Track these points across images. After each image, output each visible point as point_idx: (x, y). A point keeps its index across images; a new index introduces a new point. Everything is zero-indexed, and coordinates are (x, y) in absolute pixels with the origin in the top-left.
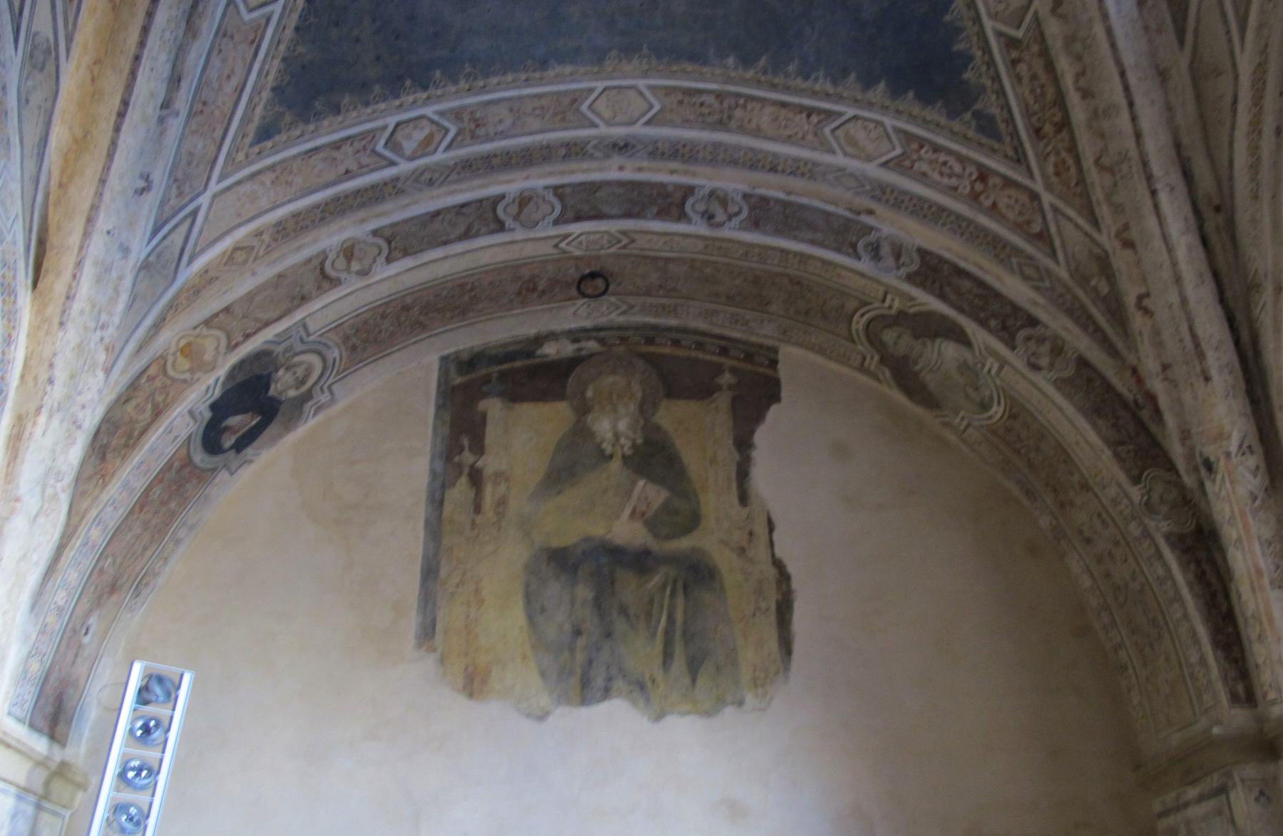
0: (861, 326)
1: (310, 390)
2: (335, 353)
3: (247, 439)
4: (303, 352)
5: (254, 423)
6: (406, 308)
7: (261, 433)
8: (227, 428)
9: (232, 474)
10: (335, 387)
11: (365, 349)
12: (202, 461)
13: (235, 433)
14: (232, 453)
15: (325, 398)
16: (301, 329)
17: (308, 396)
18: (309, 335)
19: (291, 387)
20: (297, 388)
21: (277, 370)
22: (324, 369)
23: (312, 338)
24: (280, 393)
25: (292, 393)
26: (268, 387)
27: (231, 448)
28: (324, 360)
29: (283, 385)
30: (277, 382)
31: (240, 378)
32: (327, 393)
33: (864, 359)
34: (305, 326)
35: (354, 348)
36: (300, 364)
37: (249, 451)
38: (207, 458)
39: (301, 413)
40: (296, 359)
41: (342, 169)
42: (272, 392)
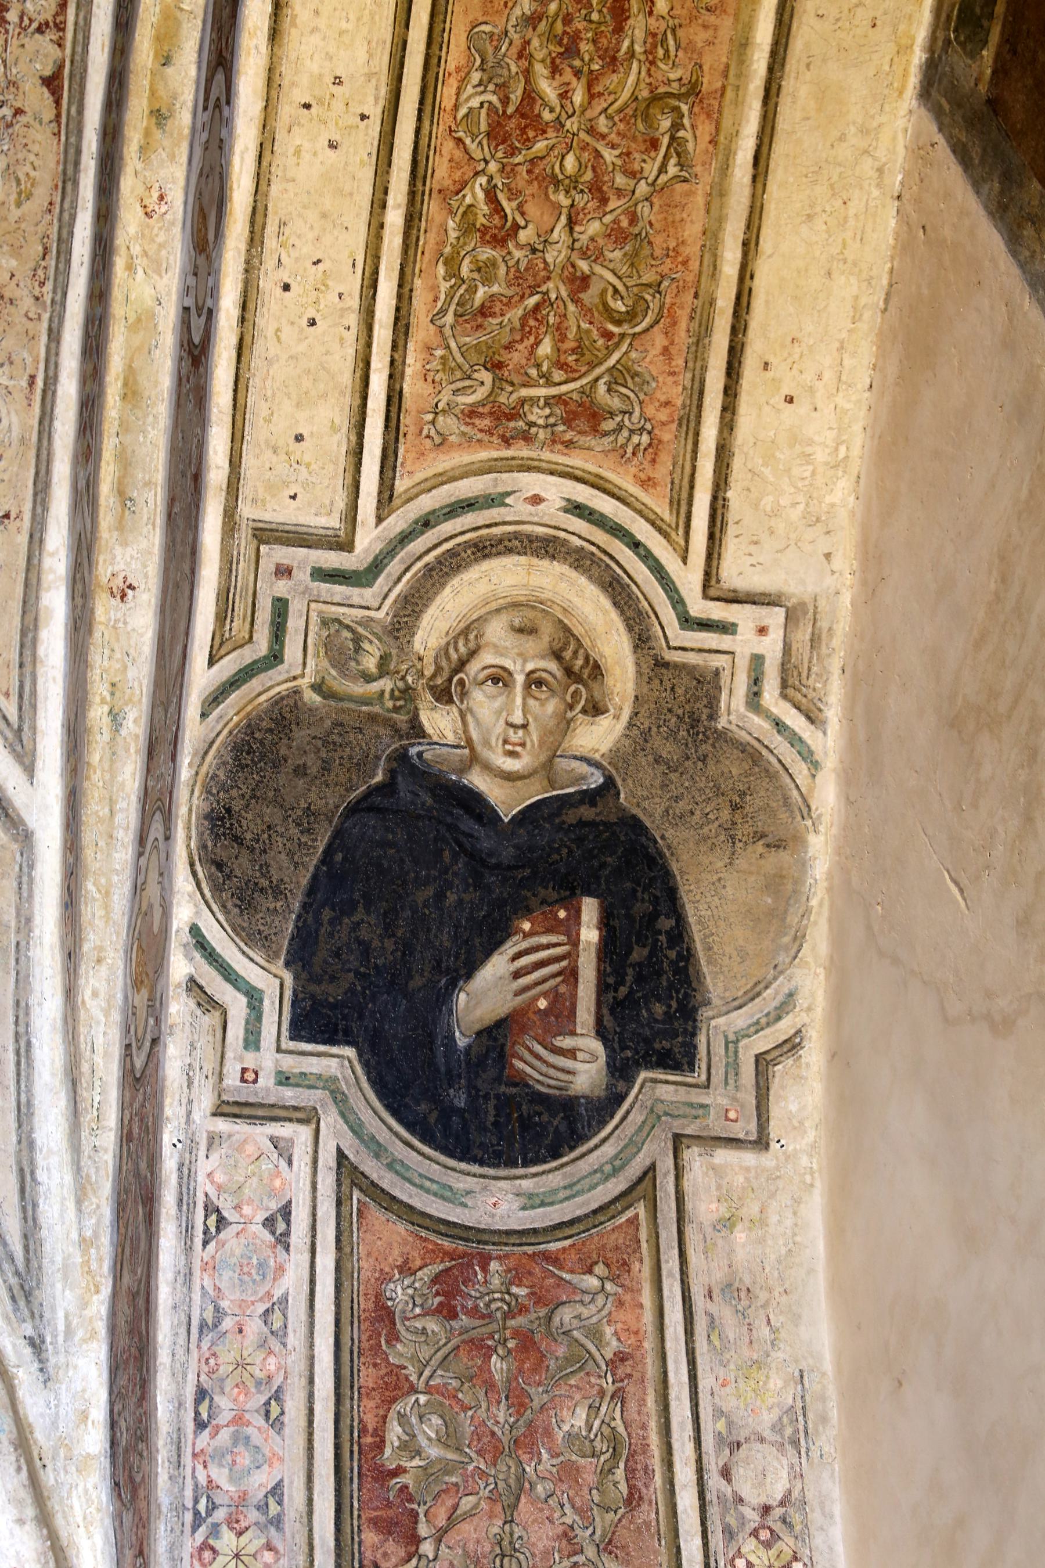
1: (656, 667)
2: (542, 496)
3: (654, 1006)
4: (412, 606)
5: (590, 935)
6: (514, 124)
7: (679, 934)
8: (497, 1036)
9: (761, 1143)
10: (735, 572)
12: (531, 1201)
13: (561, 1015)
14: (655, 1088)
15: (756, 636)
16: (275, 554)
18: (346, 545)
19: (566, 725)
20: (595, 709)
21: (417, 730)
22: (581, 560)
23: (368, 539)
26: (473, 804)
28: (547, 547)
29: (501, 746)
30: (474, 759)
32: (742, 615)
34: (266, 534)
35: (584, 416)
36: (468, 635)
38: (549, 1178)
39: (752, 754)
40: (431, 633)
41: (36, 99)
42: (505, 800)
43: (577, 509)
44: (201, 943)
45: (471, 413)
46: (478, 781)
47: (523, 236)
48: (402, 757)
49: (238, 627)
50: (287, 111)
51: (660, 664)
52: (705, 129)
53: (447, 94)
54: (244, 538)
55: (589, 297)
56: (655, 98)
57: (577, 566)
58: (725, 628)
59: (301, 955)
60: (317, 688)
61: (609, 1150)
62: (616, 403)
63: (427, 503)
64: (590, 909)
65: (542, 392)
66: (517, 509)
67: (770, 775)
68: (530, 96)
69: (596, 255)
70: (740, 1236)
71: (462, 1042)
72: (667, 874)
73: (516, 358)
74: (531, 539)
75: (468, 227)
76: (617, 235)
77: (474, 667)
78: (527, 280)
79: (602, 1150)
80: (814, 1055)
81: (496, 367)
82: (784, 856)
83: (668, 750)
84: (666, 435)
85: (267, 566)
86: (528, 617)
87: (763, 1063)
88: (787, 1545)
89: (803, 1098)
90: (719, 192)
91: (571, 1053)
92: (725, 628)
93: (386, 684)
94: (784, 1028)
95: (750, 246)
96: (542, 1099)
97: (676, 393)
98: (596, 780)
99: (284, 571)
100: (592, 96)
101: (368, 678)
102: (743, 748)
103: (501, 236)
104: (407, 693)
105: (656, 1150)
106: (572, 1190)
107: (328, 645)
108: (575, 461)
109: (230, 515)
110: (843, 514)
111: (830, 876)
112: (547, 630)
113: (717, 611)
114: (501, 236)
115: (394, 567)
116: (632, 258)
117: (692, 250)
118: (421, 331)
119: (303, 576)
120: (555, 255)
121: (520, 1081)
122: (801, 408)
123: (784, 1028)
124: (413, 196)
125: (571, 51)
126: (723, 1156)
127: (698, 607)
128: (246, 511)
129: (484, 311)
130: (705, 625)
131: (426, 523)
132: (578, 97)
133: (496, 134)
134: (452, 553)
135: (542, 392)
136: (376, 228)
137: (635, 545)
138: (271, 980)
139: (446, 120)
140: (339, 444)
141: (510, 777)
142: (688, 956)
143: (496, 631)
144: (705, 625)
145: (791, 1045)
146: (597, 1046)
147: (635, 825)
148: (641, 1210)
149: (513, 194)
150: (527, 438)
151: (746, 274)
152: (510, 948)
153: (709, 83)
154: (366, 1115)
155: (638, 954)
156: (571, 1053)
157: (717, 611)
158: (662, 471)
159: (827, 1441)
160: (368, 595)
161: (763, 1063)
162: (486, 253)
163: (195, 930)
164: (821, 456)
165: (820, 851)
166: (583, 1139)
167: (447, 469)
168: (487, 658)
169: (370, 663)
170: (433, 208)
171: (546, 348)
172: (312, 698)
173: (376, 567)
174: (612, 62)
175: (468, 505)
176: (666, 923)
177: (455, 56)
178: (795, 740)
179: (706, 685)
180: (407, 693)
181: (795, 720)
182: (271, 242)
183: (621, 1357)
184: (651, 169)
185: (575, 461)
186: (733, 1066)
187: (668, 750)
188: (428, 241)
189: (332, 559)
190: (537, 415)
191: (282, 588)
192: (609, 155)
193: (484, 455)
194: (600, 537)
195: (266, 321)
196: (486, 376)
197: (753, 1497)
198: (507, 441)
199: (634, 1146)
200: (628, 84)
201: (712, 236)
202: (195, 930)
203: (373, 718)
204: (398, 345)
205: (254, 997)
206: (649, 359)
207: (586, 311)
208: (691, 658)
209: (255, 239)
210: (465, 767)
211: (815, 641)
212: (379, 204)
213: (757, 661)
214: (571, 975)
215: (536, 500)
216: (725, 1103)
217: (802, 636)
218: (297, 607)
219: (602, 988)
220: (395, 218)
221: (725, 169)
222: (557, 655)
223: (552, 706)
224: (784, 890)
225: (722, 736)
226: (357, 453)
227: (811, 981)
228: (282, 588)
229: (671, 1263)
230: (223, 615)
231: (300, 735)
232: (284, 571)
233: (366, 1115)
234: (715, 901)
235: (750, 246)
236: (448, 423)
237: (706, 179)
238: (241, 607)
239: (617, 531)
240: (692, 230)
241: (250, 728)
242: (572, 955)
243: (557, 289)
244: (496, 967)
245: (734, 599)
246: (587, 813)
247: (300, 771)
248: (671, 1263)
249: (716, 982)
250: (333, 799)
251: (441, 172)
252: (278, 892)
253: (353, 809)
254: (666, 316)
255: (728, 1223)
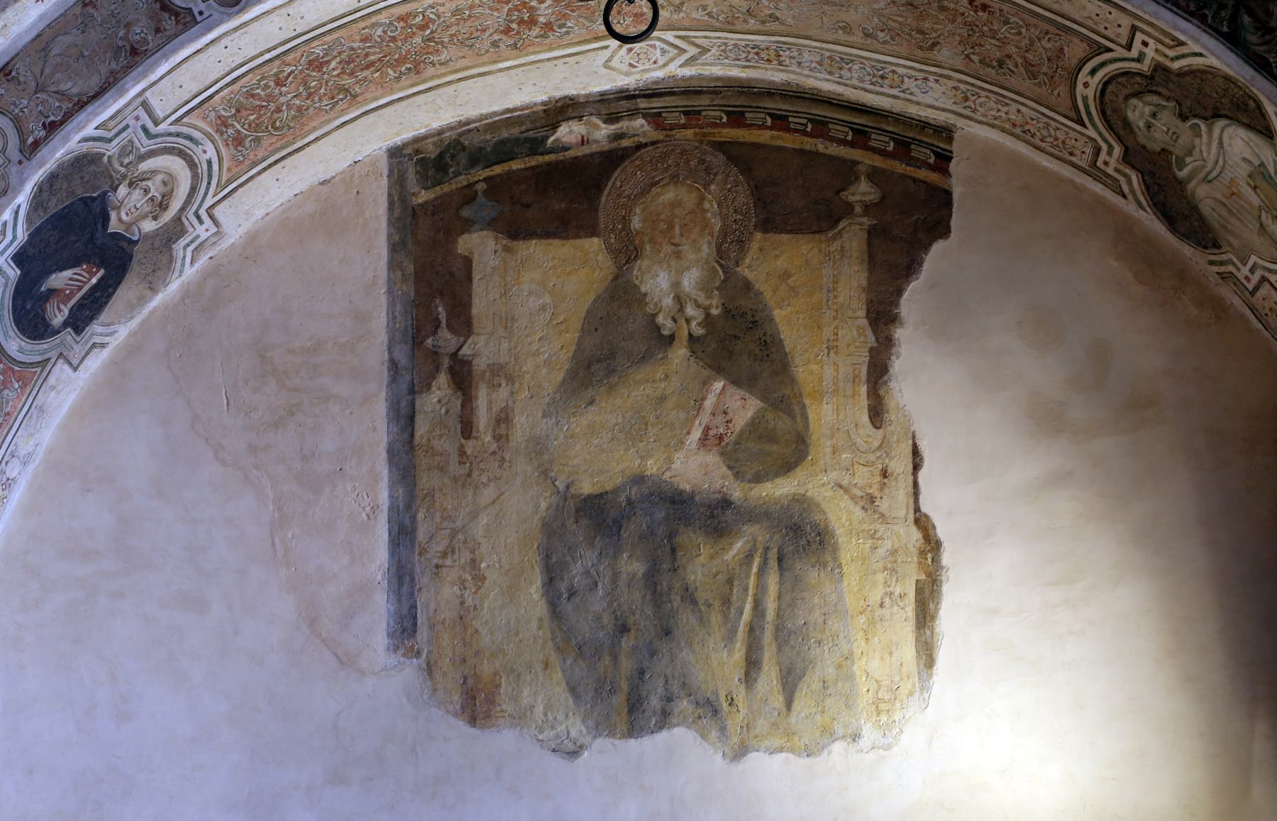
0: (1090, 93)
1: (178, 219)
3: (87, 312)
4: (152, 154)
5: (94, 281)
6: (317, 64)
7: (110, 296)
8: (52, 292)
9: (75, 369)
10: (218, 212)
11: (257, 140)
12: (21, 351)
15: (204, 230)
16: (141, 112)
17: (176, 230)
18: (156, 124)
19: (145, 217)
20: (155, 218)
21: (115, 189)
22: (195, 177)
23: (163, 127)
24: (129, 226)
25: (148, 226)
26: (106, 219)
27: (66, 324)
28: (192, 165)
29: (129, 211)
30: (118, 208)
31: (54, 207)
33: (1097, 151)
34: (145, 105)
35: (238, 141)
36: (154, 172)
37: (96, 327)
38: (27, 344)
39: (171, 260)
40: (145, 166)
42: (114, 226)
43: (209, 163)
44: (17, 213)
45: (219, 117)
46: (113, 215)
47: (284, 89)
48: (105, 193)
49: (112, 123)
50: (284, 11)
51: (180, 219)
52: (345, 106)
53: (316, 43)
54: (140, 100)
55: (276, 116)
56: (347, 90)
57: (192, 177)
58: (201, 222)
59: (34, 236)
60: (109, 157)
61: (45, 346)
62: (247, 145)
63: (185, 130)
64: (102, 272)
65: (239, 127)
66: (198, 150)
67: (169, 270)
68: (328, 62)
69: (289, 107)
70: (53, 394)
71: (43, 289)
72: (123, 277)
73: (244, 113)
74: (193, 160)
75: (276, 75)
76: (299, 109)
77: (145, 183)
78: (270, 98)
79: (43, 346)
80: (105, 354)
81: (238, 111)
82: (150, 293)
83: (157, 243)
84: (247, 162)
85: (135, 114)
86: (170, 183)
87: (94, 345)
88: (6, 492)
89: (95, 363)
90: (328, 122)
91: (60, 311)
92: (201, 222)
93: (123, 170)
94: (106, 339)
95: (317, 139)
96: (44, 319)
97: (260, 155)
98: (135, 238)
99: (137, 118)
100: (338, 76)
101: (122, 165)
102: (171, 256)
103: (279, 83)
104: (124, 177)
105: (53, 354)
106: (31, 353)
107: (124, 148)
108: (223, 150)
109: (144, 90)
110: (254, 219)
111: (155, 308)
112: (169, 188)
113: (204, 216)
114: (279, 83)
115: (159, 140)
116: (294, 117)
117: (307, 128)
118: (235, 87)
119: (140, 123)
120: (283, 100)
121: (44, 311)
122: (277, 184)
123: (106, 339)
124: (278, 56)
125: (348, 63)
126: (66, 367)
127: (202, 212)
128: (148, 94)
129: (253, 96)
130: (198, 217)
131: (178, 135)
132: (335, 73)
133: (310, 63)
134: (174, 148)
135: (239, 127)
136: (261, 54)
137: (209, 183)
138: (22, 235)
139: (307, 48)
140: (187, 96)
141: (120, 220)
142: (106, 303)
143: (159, 178)
144: (198, 217)
145: (103, 345)
146: (66, 312)
147: (131, 257)
148: (39, 370)
149: (295, 78)
150: (222, 134)
151: (308, 145)
152: (77, 270)
153: (359, 99)
154: (7, 296)
155: (98, 294)
156: (60, 311)
157: (204, 216)
158: (235, 170)
159: (31, 468)
160: (145, 141)
161: (94, 345)
162: (272, 84)
163: (19, 206)
164: (266, 199)
165: (157, 301)
166: (43, 338)
167: (199, 125)
168: (149, 183)
169: (126, 161)
170: (277, 63)
171: (252, 118)
172: (105, 159)
173: (156, 136)
174: (352, 74)
175: (190, 138)
176: (111, 290)
177: (328, 38)
178: (183, 265)
179: (182, 232)
180: (124, 177)
181: (188, 260)
182: (238, 34)
183: (8, 414)
184: (325, 103)
185: (223, 150)
186: (87, 341)
187: (157, 243)
188: (266, 68)
189: (150, 125)
190: (231, 131)
191: (132, 123)
192: (322, 91)
193: (209, 130)
194: (205, 174)
195: (211, 50)
196: (233, 111)
197: (8, 474)
198: (217, 131)
199: (51, 349)
200: (347, 81)
201: (315, 129)
202: (19, 206)
203: (111, 177)
204: (227, 85)
205: (15, 238)
206: (266, 142)
207: (271, 118)
208: (186, 223)
209: (236, 29)
210: (113, 209)
211: (214, 243)
212: (269, 51)
213: (198, 236)
214: (80, 288)
215: (205, 152)
216: (78, 350)
217: (213, 240)
218: (129, 130)
219: (83, 298)
220: (267, 56)
221: (336, 118)
222: (163, 196)
223: (148, 209)
224: (142, 301)
225: (171, 249)
226: (187, 102)
227: (123, 332)
228: (132, 123)
229: (34, 392)
230: (112, 118)
231: (93, 167)
232: (137, 118)
233: (7, 296)
234: (125, 293)
235: (317, 139)
236: (213, 114)
237: (332, 115)
238: (118, 119)
239: (210, 177)
240: (313, 124)
241: (85, 156)
242: (85, 283)
243: (272, 106)
244: (68, 273)
245: (211, 217)
246: (125, 245)
247: (82, 178)
248: (34, 392)
249: (104, 316)
250: (80, 193)
251: (290, 58)
252: (45, 211)
253: (81, 199)
254: (283, 136)
255: (53, 388)
